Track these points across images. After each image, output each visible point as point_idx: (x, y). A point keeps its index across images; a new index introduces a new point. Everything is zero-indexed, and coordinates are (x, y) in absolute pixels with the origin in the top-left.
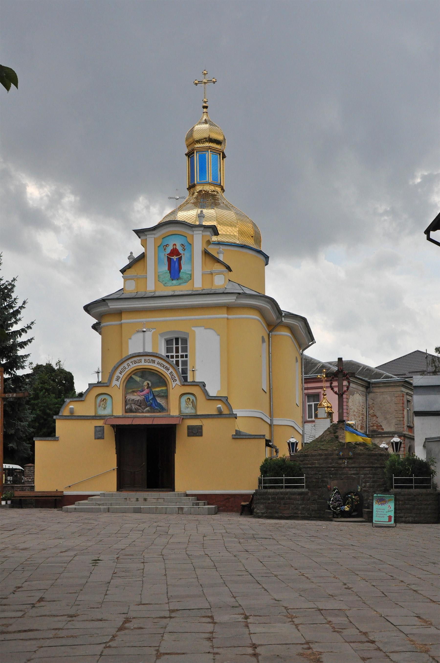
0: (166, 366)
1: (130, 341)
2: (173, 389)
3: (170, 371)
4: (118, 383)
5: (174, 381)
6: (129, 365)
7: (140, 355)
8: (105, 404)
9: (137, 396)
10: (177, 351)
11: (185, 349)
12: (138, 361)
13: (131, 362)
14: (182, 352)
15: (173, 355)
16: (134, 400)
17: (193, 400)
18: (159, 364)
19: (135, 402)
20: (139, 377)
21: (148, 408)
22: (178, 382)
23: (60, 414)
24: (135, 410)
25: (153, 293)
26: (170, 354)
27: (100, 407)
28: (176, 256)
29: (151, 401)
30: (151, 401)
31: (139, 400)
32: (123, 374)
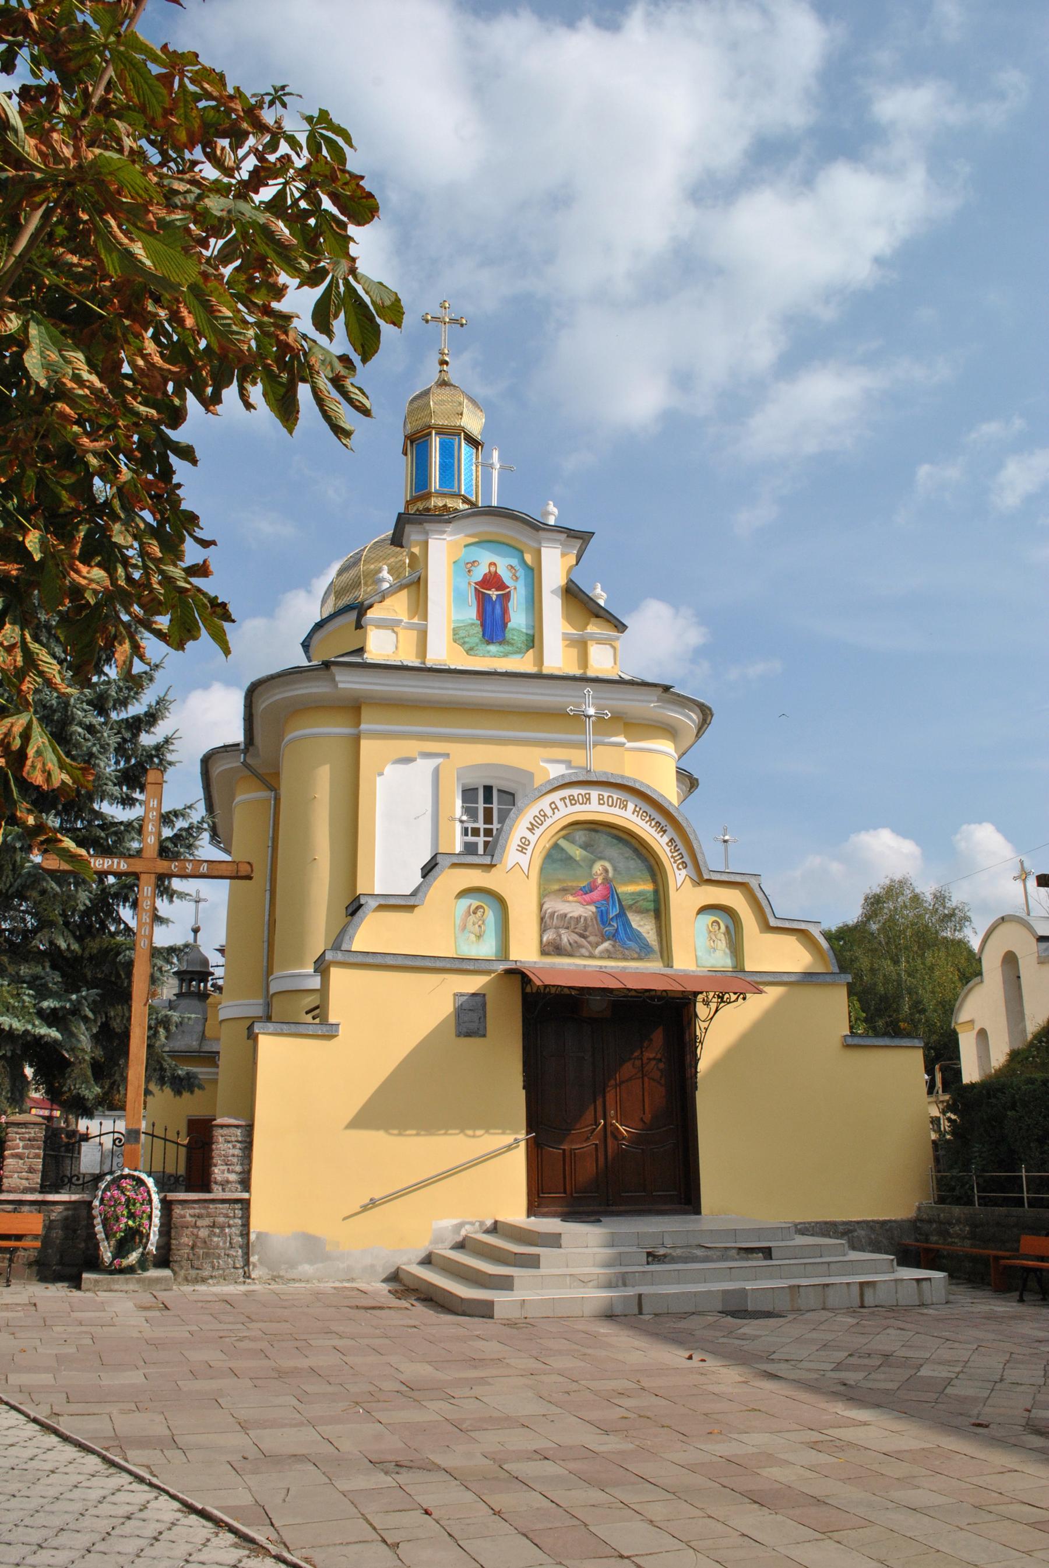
1: (379, 779)
6: (556, 807)
7: (589, 779)
8: (480, 922)
9: (574, 904)
12: (580, 796)
13: (561, 800)
16: (565, 916)
19: (569, 923)
20: (581, 847)
21: (606, 945)
24: (569, 948)
27: (466, 931)
28: (497, 590)
32: (538, 832)
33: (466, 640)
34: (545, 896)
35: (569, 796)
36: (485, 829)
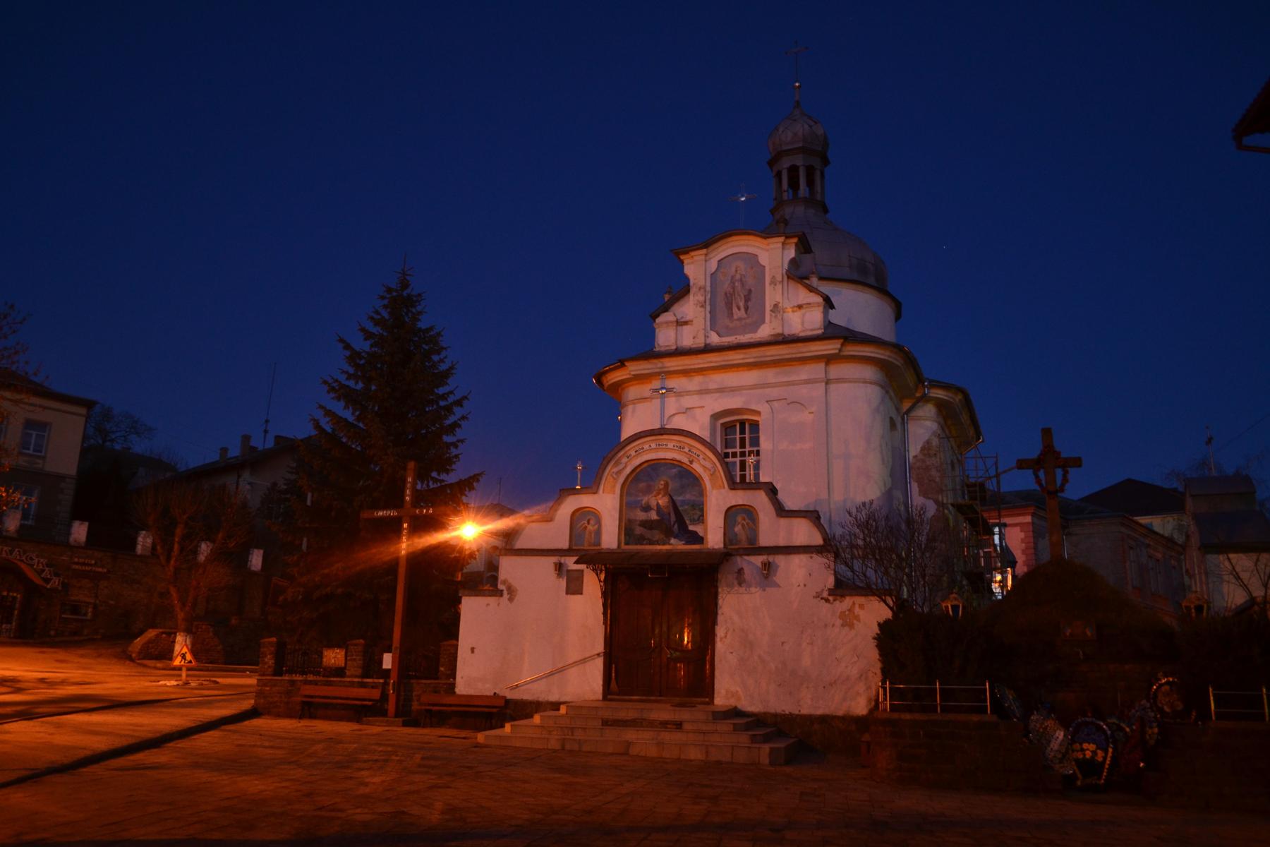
10: (743, 445)
11: (755, 441)
14: (751, 446)
15: (736, 452)
26: (730, 451)
36: (745, 452)
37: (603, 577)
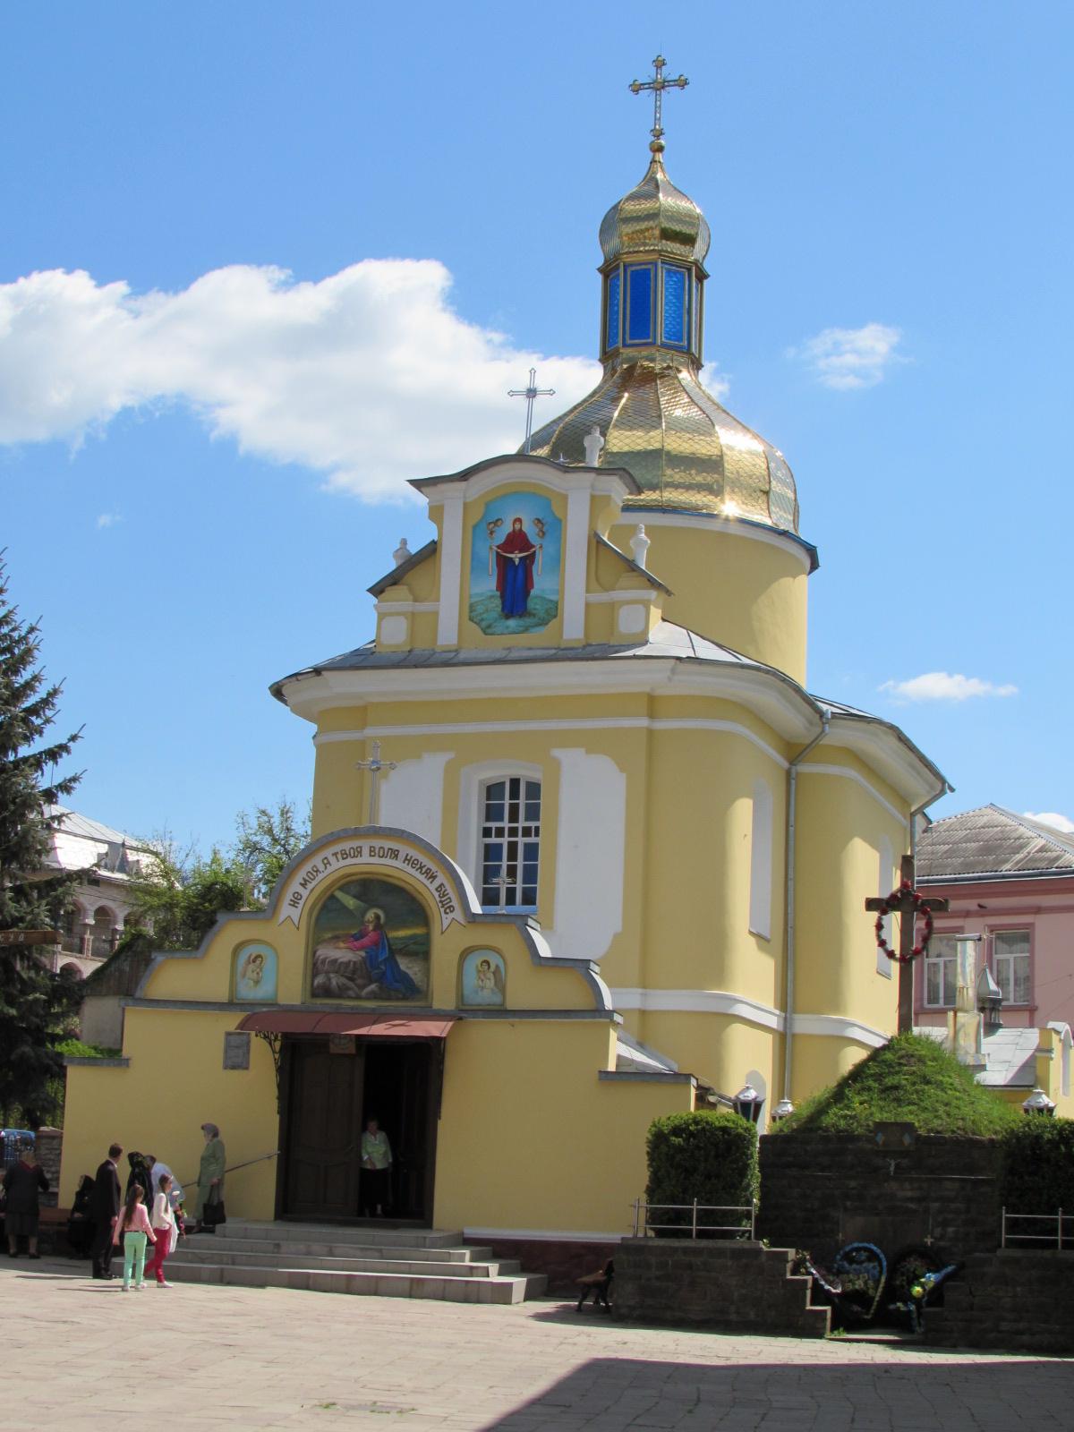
0: (428, 869)
2: (442, 933)
3: (437, 883)
4: (295, 913)
5: (448, 911)
6: (329, 863)
9: (344, 950)
10: (514, 817)
11: (533, 812)
12: (352, 851)
13: (333, 855)
16: (335, 961)
17: (497, 966)
18: (409, 861)
19: (339, 968)
20: (355, 897)
21: (373, 987)
22: (458, 914)
23: (138, 994)
25: (453, 654)
26: (494, 825)
28: (520, 552)
29: (383, 967)
30: (383, 967)
31: (350, 961)
32: (310, 886)
33: (485, 616)
34: (318, 943)
35: (341, 851)
36: (517, 828)
37: (278, 1045)
